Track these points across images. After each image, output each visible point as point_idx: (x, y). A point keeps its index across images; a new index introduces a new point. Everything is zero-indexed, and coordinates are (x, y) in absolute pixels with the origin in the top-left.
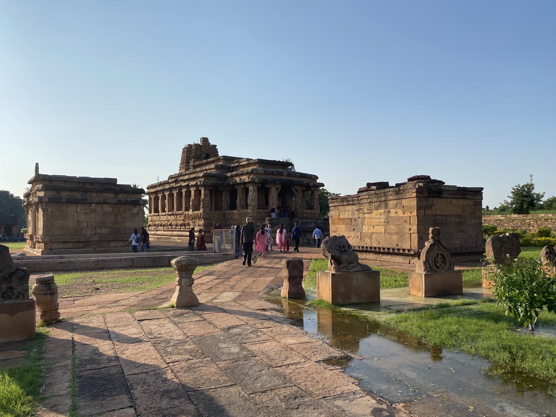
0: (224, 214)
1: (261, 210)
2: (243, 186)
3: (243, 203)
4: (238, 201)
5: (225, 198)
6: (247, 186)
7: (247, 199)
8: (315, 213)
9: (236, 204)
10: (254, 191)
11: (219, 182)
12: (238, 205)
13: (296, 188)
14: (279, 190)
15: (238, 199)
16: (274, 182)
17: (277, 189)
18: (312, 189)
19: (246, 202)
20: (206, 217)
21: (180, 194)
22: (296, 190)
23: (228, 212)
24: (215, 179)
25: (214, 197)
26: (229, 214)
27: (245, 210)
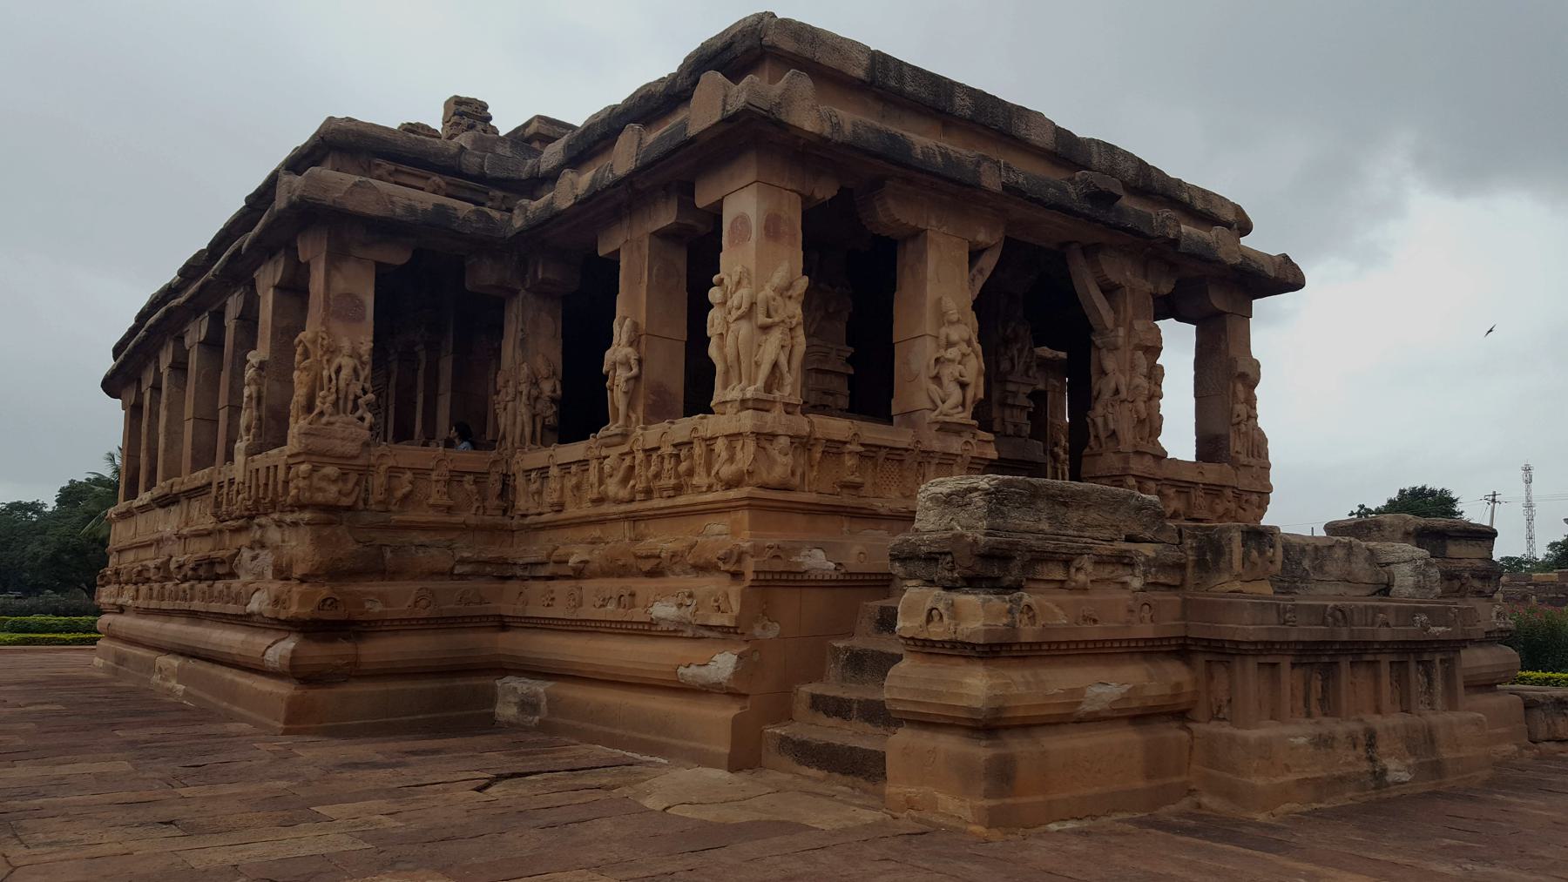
0: (506, 478)
1: (838, 427)
2: (665, 216)
3: (676, 383)
4: (619, 351)
5: (527, 360)
6: (703, 200)
7: (698, 309)
8: (1238, 494)
9: (599, 382)
10: (772, 229)
11: (464, 208)
12: (617, 397)
13: (1114, 277)
14: (989, 262)
15: (621, 332)
16: (954, 191)
17: (975, 255)
18: (1218, 301)
19: (697, 339)
20: (331, 493)
21: (213, 343)
22: (1110, 290)
23: (537, 457)
24: (436, 179)
25: (446, 366)
26: (543, 471)
27: (683, 427)
